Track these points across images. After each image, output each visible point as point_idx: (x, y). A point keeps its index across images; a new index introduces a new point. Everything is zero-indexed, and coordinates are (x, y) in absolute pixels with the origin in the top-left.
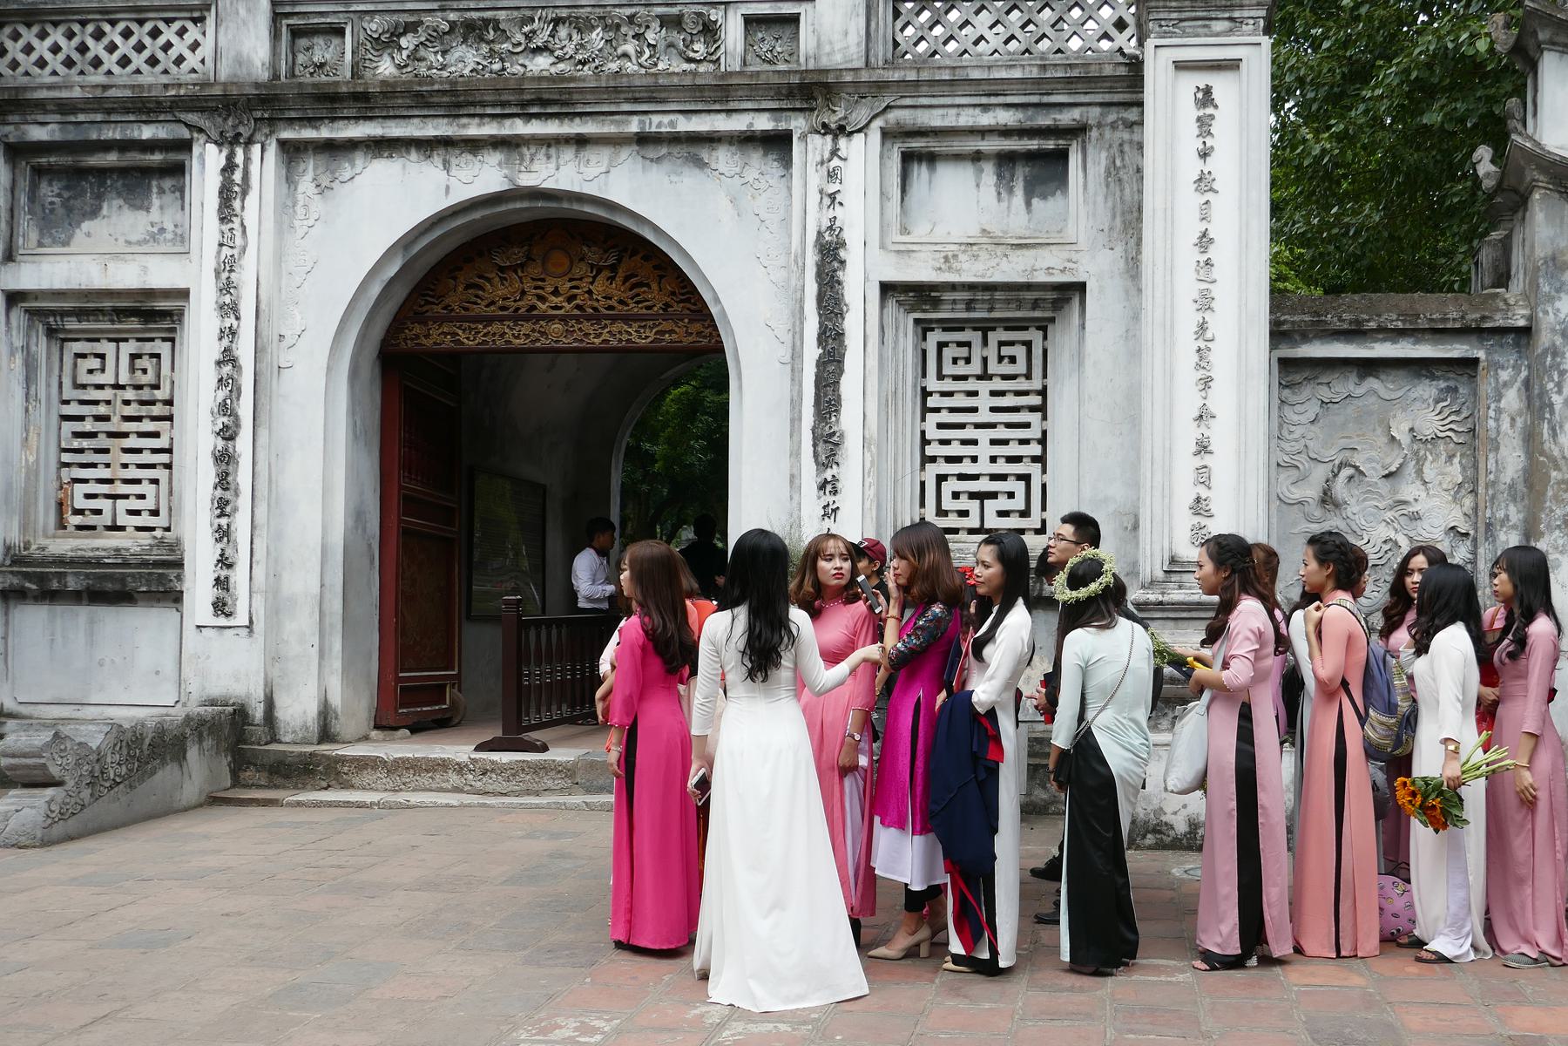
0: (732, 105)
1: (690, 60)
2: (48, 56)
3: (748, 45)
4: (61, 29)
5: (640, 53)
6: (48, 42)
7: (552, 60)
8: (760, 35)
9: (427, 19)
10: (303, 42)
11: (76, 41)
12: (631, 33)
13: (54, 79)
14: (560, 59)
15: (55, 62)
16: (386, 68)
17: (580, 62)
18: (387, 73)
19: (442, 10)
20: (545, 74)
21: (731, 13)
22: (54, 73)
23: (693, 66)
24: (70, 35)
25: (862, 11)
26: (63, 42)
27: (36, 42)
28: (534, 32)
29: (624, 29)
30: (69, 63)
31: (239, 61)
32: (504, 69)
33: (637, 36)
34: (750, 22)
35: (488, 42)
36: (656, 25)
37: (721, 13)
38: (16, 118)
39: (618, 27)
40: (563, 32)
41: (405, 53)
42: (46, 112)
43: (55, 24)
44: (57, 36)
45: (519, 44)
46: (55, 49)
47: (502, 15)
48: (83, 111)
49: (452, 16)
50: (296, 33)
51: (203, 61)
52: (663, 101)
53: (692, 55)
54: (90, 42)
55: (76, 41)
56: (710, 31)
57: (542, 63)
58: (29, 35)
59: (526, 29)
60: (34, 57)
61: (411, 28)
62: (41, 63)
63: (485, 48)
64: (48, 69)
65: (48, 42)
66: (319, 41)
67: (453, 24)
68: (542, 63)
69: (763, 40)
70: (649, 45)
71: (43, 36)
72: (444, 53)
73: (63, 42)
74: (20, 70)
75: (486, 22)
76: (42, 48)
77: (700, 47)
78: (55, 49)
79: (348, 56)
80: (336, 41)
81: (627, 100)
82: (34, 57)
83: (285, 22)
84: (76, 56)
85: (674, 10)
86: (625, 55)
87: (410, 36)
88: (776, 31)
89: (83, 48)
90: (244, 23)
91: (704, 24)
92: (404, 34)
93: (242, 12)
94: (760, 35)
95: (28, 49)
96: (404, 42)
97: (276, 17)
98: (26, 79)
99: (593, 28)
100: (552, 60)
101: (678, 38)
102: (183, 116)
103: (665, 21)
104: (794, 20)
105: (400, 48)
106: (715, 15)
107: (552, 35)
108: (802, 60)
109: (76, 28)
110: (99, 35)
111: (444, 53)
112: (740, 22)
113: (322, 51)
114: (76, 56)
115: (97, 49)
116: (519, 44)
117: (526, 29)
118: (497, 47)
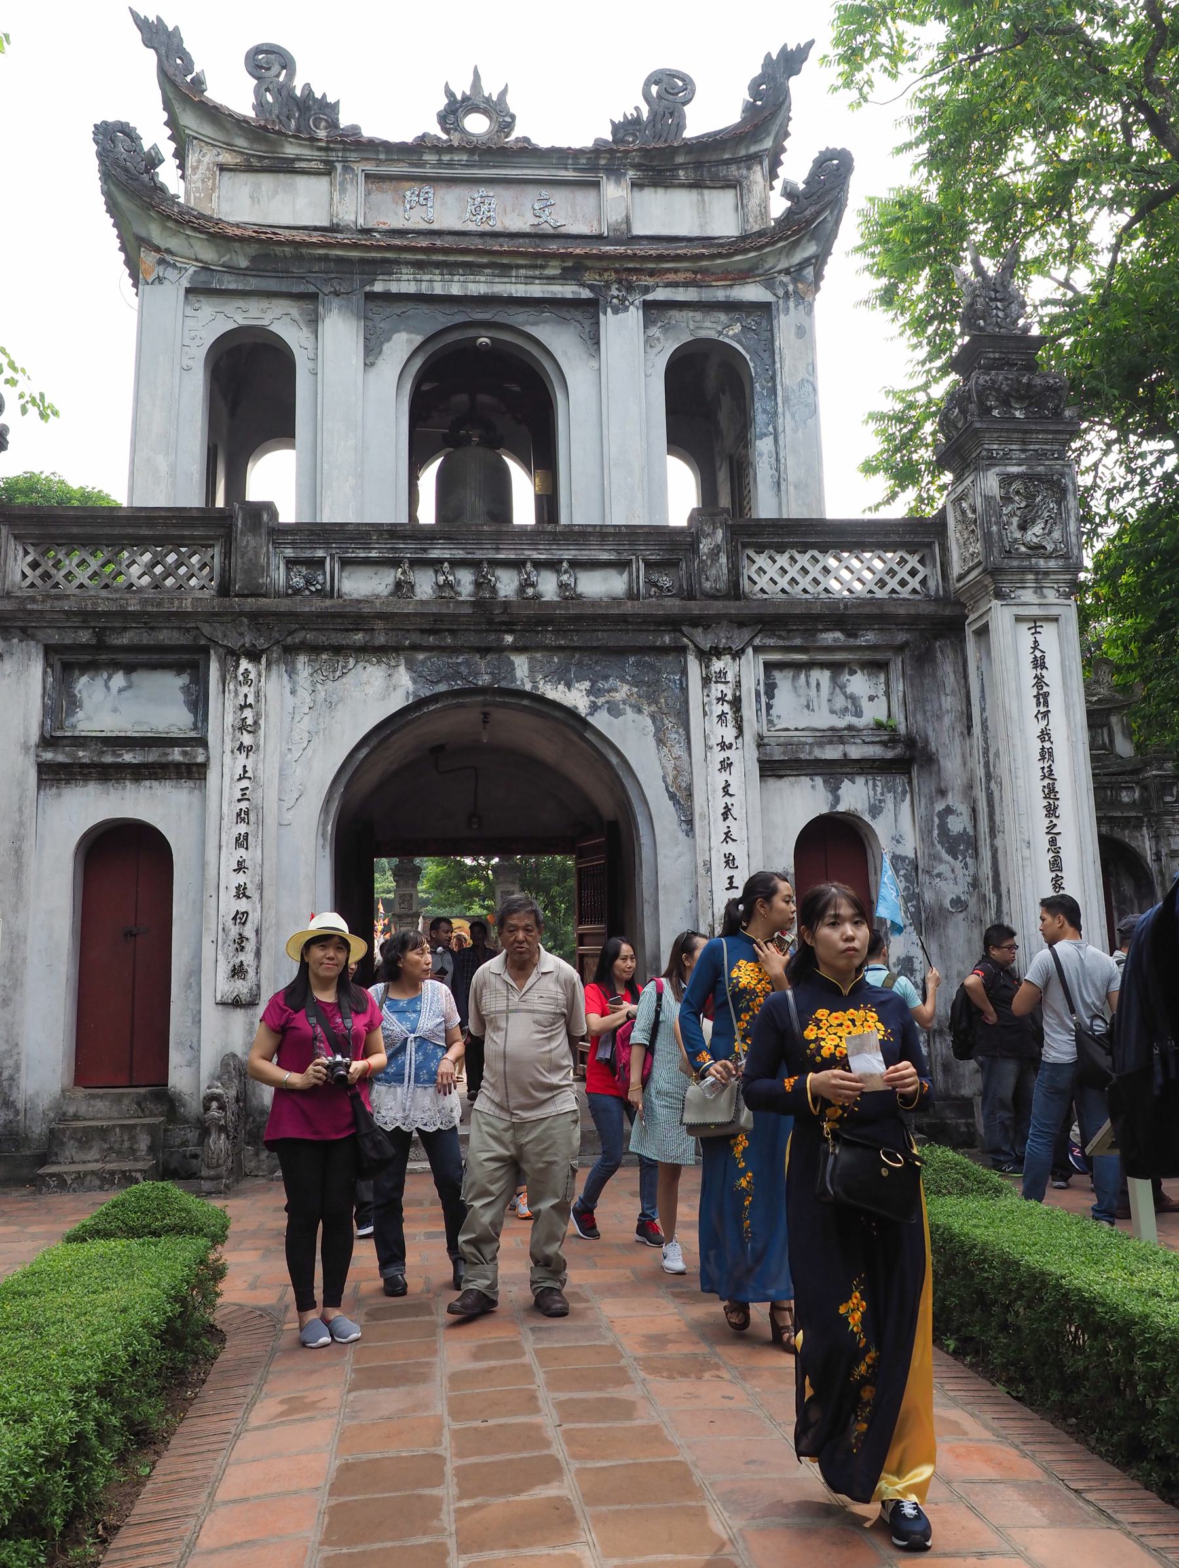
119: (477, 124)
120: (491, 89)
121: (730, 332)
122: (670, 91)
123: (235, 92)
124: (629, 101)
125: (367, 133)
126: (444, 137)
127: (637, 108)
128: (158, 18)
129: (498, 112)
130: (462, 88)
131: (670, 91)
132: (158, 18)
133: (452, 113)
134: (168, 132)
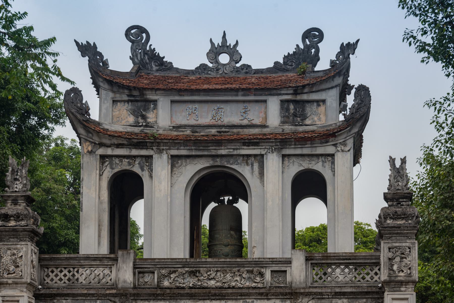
0: (269, 297)
1: (256, 282)
2: (63, 278)
3: (272, 278)
4: (67, 270)
5: (241, 280)
6: (63, 274)
7: (215, 282)
8: (275, 275)
9: (179, 270)
10: (141, 275)
11: (71, 274)
12: (238, 274)
13: (64, 285)
14: (218, 281)
15: (65, 279)
16: (166, 283)
17: (224, 283)
18: (167, 284)
19: (183, 267)
20: (214, 286)
21: (267, 270)
22: (65, 283)
23: (256, 284)
24: (69, 272)
25: (305, 270)
26: (67, 274)
27: (59, 274)
28: (211, 274)
29: (236, 273)
30: (69, 280)
31: (125, 281)
32: (201, 284)
33: (240, 275)
34: (272, 271)
35: (197, 277)
36: (245, 272)
37: (265, 270)
38: (59, 298)
39: (234, 273)
40: (219, 274)
41: (172, 279)
42: (69, 296)
43: (65, 268)
44: (65, 272)
45: (206, 277)
46: (65, 275)
47: (201, 269)
48: (81, 296)
49: (187, 269)
50: (140, 273)
51: (111, 280)
52: (249, 296)
53: (256, 281)
54: (76, 274)
55: (71, 274)
56: (262, 275)
57: (212, 283)
58: (56, 271)
59: (209, 273)
60: (58, 278)
61: (175, 272)
62: (61, 280)
63: (196, 279)
64: (63, 282)
65: (63, 274)
66: (147, 275)
67: (187, 272)
68: (212, 283)
69: (276, 277)
70: (243, 278)
71: (61, 271)
72: (183, 279)
73: (67, 274)
74: (54, 282)
75: (197, 271)
76: (61, 275)
77: (258, 279)
78: (65, 275)
79: (156, 280)
80: (151, 275)
81: (239, 296)
82: (58, 278)
83: (137, 270)
84: (71, 278)
85: (251, 269)
86: (237, 280)
87: (173, 274)
88: (280, 274)
89: (73, 275)
90: (126, 271)
91: (259, 272)
92: (172, 273)
93: (125, 267)
94: (275, 275)
95: (57, 275)
96: (172, 276)
97: (135, 268)
98: (56, 284)
99: (227, 273)
100: (215, 282)
101: (252, 276)
102: (110, 298)
103: (248, 272)
104: (285, 271)
105: (171, 278)
106: (263, 270)
107: (216, 275)
108: (288, 283)
109: (72, 269)
110: (78, 272)
111: (183, 279)
112: (270, 272)
113: (147, 278)
114: (71, 278)
115: (77, 275)
116: (206, 277)
117: (209, 273)
118: (200, 278)
119: (224, 59)
120: (231, 42)
121: (318, 166)
122: (313, 36)
123: (120, 60)
124: (292, 43)
125: (175, 66)
126: (210, 65)
127: (297, 45)
128: (87, 42)
129: (233, 52)
130: (218, 41)
131: (313, 36)
132: (87, 42)
133: (214, 52)
134: (93, 86)
